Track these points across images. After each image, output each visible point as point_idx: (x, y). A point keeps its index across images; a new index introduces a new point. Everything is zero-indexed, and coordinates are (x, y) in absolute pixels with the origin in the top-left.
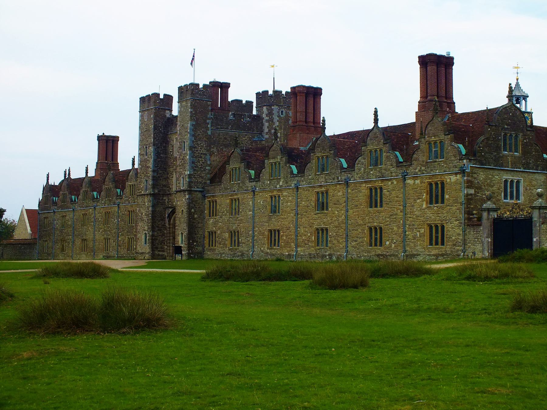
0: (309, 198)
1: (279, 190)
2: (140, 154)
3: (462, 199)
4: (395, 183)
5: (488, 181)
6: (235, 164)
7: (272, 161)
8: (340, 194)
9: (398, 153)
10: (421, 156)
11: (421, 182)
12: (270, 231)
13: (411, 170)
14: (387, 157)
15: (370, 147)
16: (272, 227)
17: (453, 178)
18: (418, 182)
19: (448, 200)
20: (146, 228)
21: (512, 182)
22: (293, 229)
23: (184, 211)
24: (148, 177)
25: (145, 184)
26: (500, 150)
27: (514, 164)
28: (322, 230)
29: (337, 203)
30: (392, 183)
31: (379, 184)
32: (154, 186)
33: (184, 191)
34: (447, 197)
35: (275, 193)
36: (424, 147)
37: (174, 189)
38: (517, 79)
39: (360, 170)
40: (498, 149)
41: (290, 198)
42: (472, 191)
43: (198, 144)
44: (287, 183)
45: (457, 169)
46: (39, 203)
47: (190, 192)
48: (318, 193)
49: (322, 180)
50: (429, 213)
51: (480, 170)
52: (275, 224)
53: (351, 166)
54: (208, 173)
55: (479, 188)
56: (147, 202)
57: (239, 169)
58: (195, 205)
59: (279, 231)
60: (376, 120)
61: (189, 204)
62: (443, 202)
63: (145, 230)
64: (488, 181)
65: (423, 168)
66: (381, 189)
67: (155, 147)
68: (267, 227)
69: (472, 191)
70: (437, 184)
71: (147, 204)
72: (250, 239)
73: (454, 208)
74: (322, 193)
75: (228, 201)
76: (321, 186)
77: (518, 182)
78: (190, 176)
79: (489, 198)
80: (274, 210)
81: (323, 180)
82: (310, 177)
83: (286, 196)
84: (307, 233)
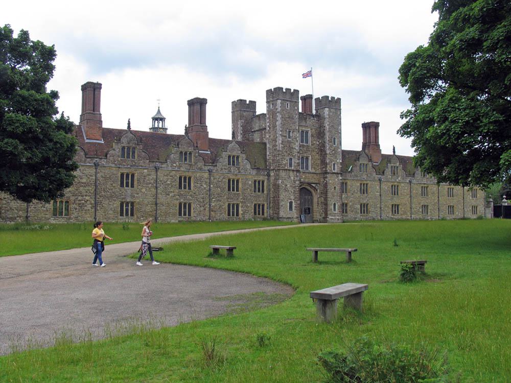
0: (417, 189)
1: (399, 182)
2: (189, 123)
7: (393, 165)
8: (435, 189)
16: (394, 203)
20: (292, 197)
22: (409, 205)
28: (425, 206)
29: (433, 193)
33: (338, 174)
35: (396, 184)
38: (159, 107)
49: (425, 181)
50: (473, 201)
52: (396, 201)
59: (398, 206)
60: (394, 152)
63: (291, 199)
68: (390, 203)
71: (292, 178)
72: (379, 210)
75: (359, 184)
84: (417, 207)
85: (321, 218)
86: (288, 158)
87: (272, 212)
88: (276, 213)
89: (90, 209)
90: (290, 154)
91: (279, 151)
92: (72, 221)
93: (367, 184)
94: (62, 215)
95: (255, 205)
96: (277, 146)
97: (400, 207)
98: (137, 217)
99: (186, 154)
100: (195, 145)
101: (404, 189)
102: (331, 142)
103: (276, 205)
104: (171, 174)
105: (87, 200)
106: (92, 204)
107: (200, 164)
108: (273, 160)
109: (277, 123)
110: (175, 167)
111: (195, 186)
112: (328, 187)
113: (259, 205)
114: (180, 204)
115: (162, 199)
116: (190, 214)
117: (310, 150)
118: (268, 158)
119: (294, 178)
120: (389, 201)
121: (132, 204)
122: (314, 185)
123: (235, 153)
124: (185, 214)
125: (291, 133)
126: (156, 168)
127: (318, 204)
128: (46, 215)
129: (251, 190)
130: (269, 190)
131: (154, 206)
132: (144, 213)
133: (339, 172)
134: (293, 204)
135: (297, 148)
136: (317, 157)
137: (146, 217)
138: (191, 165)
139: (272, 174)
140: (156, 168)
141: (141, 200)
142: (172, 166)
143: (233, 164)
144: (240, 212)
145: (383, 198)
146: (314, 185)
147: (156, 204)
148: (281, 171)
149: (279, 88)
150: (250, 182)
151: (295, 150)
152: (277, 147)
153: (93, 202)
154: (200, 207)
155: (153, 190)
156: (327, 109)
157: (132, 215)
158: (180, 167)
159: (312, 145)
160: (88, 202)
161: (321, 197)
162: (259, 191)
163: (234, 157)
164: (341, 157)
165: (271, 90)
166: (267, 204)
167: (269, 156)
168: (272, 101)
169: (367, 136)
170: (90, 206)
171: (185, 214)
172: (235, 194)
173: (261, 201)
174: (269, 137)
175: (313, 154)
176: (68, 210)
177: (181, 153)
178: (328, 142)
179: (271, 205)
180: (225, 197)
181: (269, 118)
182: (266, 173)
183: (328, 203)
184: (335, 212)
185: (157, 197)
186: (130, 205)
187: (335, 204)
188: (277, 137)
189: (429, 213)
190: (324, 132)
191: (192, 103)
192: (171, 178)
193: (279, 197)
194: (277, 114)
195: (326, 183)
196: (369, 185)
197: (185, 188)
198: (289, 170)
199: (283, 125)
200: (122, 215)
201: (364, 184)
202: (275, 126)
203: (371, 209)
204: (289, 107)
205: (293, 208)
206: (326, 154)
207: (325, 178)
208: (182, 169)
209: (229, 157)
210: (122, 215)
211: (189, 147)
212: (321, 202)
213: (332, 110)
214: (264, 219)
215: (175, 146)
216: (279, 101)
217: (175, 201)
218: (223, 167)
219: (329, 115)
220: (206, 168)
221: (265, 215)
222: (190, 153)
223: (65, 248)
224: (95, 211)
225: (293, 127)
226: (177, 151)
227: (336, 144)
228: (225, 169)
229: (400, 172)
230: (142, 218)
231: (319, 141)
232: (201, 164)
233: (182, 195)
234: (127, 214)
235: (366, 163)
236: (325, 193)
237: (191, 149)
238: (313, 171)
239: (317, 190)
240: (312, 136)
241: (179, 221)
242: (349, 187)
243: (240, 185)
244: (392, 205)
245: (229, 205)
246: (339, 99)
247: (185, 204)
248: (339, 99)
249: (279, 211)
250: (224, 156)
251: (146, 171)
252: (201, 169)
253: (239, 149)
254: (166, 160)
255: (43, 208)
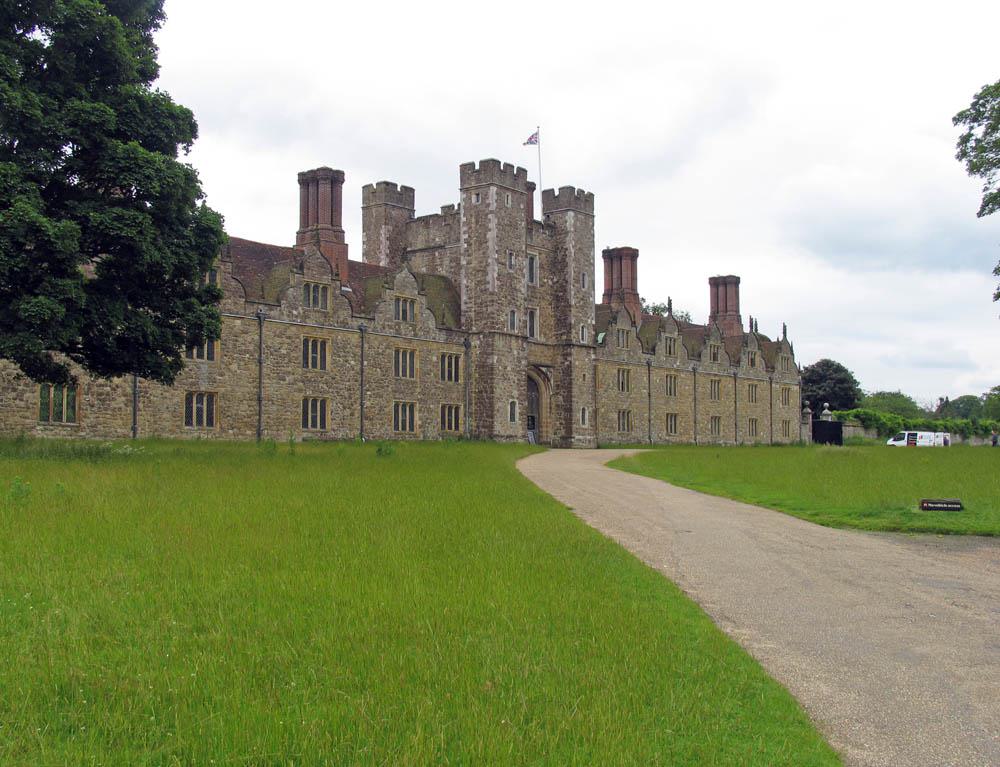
0: (704, 386)
1: (677, 370)
7: (668, 335)
12: (667, 414)
16: (670, 411)
20: (515, 393)
22: (691, 414)
23: (587, 376)
24: (518, 307)
33: (587, 347)
35: (673, 373)
52: (673, 408)
63: (513, 397)
68: (664, 410)
75: (616, 371)
80: (671, 392)
85: (557, 437)
86: (508, 310)
87: (474, 424)
88: (484, 427)
89: (122, 405)
90: (512, 301)
91: (492, 294)
92: (83, 434)
93: (628, 371)
94: (60, 419)
95: (443, 407)
96: (489, 283)
97: (679, 419)
98: (221, 428)
99: (316, 287)
100: (335, 271)
101: (685, 383)
102: (577, 281)
103: (485, 408)
104: (288, 333)
105: (117, 386)
106: (125, 395)
107: (344, 314)
108: (477, 313)
109: (490, 235)
110: (296, 317)
111: (334, 362)
112: (574, 374)
113: (450, 408)
114: (306, 401)
115: (271, 388)
116: (323, 425)
117: (538, 295)
118: (463, 307)
119: (519, 353)
120: (662, 409)
121: (211, 396)
122: (544, 369)
123: (407, 294)
124: (314, 425)
125: (513, 257)
126: (259, 318)
127: (551, 408)
128: (26, 418)
129: (435, 376)
130: (468, 376)
131: (254, 403)
132: (234, 420)
133: (591, 344)
134: (517, 405)
135: (523, 290)
136: (550, 311)
137: (239, 429)
138: (326, 315)
139: (475, 342)
140: (259, 318)
141: (229, 389)
142: (290, 314)
143: (405, 318)
144: (417, 422)
145: (653, 400)
146: (544, 369)
147: (259, 400)
148: (497, 337)
149: (493, 160)
150: (434, 359)
151: (519, 295)
152: (489, 286)
153: (129, 390)
154: (344, 408)
155: (254, 367)
156: (571, 214)
157: (210, 422)
158: (305, 317)
159: (542, 286)
160: (119, 391)
161: (557, 394)
162: (450, 378)
163: (405, 301)
164: (593, 315)
165: (472, 165)
166: (465, 406)
167: (466, 303)
168: (477, 188)
169: (615, 276)
170: (123, 399)
171: (314, 425)
172: (407, 383)
173: (454, 398)
174: (468, 264)
175: (543, 304)
176: (74, 408)
177: (307, 286)
178: (572, 281)
179: (474, 407)
180: (390, 389)
181: (467, 223)
182: (463, 339)
183: (573, 408)
184: (586, 426)
185: (260, 382)
186: (205, 399)
187: (584, 409)
188: (488, 265)
189: (722, 434)
190: (564, 260)
191: (308, 180)
192: (289, 341)
193: (492, 392)
194: (490, 216)
195: (569, 366)
196: (632, 373)
197: (314, 365)
198: (511, 335)
199: (500, 239)
200: (189, 422)
201: (623, 371)
202: (482, 242)
203: (636, 422)
204: (510, 201)
205: (517, 416)
206: (570, 306)
207: (566, 356)
208: (310, 323)
209: (398, 300)
210: (189, 422)
211: (324, 274)
212: (558, 406)
213: (579, 216)
214: (460, 438)
215: (295, 270)
216: (493, 189)
217: (295, 393)
218: (387, 323)
219: (575, 225)
220: (356, 323)
221: (461, 428)
222: (325, 289)
223: (702, 488)
224: (135, 414)
225: (517, 246)
226: (299, 283)
227: (586, 286)
228: (390, 327)
229: (679, 349)
230: (231, 431)
231: (552, 280)
232: (345, 313)
233: (310, 381)
234: (200, 422)
235: (627, 328)
236: (566, 386)
237: (326, 279)
238: (543, 340)
239: (549, 380)
240: (541, 267)
241: (304, 440)
242: (601, 376)
243: (417, 365)
244: (667, 414)
245: (397, 405)
246: (591, 196)
247: (315, 401)
248: (591, 196)
249: (493, 422)
250: (388, 299)
251: (238, 322)
252: (344, 324)
253: (415, 285)
254: (278, 301)
255: (17, 402)
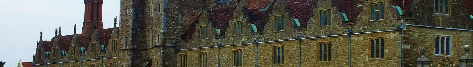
0: (267, 53)
1: (242, 46)
2: (121, 15)
3: (400, 54)
4: (342, 39)
5: (422, 38)
6: (203, 24)
7: (235, 21)
8: (294, 49)
9: (344, 14)
10: (364, 17)
11: (364, 39)
13: (355, 28)
14: (335, 17)
15: (320, 9)
17: (392, 36)
18: (361, 38)
19: (388, 54)
21: (443, 38)
23: (159, 63)
25: (126, 41)
26: (433, 11)
27: (445, 24)
30: (339, 40)
31: (328, 40)
32: (133, 42)
33: (159, 46)
34: (386, 51)
35: (238, 48)
36: (367, 8)
37: (151, 45)
39: (311, 28)
40: (430, 10)
41: (251, 53)
42: (408, 47)
43: (171, 6)
44: (248, 39)
45: (395, 28)
46: (34, 56)
47: (164, 47)
48: (275, 48)
49: (278, 37)
51: (415, 29)
53: (304, 25)
54: (180, 31)
55: (414, 44)
56: (127, 56)
57: (207, 28)
58: (168, 59)
61: (163, 58)
62: (383, 56)
64: (422, 38)
65: (366, 27)
66: (329, 44)
67: (135, 9)
69: (408, 47)
70: (377, 40)
71: (127, 57)
73: (393, 61)
74: (279, 48)
75: (197, 55)
76: (277, 42)
77: (448, 39)
78: (164, 34)
79: (423, 53)
81: (280, 37)
82: (268, 34)
83: (247, 51)
